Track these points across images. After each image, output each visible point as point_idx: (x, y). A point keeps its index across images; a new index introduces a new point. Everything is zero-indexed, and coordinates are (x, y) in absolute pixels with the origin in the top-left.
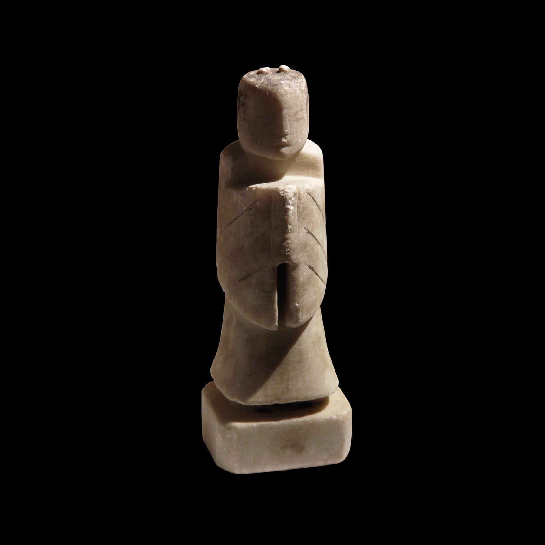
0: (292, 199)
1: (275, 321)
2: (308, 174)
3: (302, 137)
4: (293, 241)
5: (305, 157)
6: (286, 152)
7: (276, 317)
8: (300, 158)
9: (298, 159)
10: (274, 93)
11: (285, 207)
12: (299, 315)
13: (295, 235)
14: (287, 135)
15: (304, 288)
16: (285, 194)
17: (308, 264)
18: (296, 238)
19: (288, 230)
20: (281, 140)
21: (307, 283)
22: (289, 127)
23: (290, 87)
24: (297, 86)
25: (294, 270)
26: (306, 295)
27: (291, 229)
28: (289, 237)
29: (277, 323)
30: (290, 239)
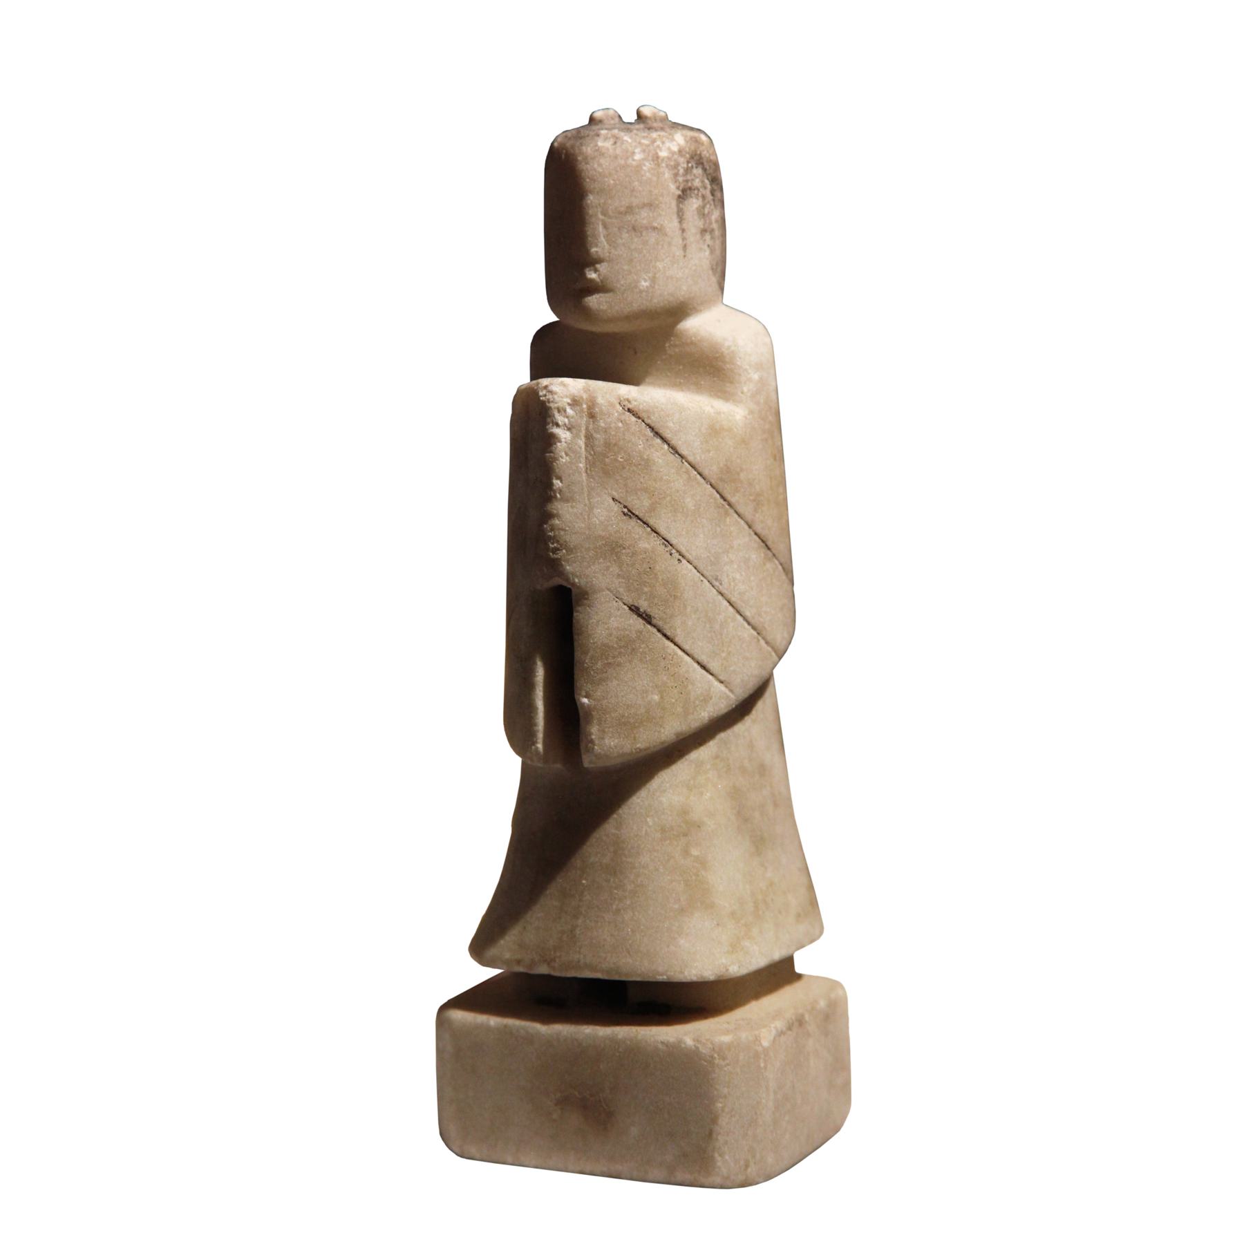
0: (565, 411)
1: (535, 739)
2: (699, 389)
3: (654, 277)
4: (570, 525)
5: (689, 341)
6: (597, 307)
7: (536, 728)
8: (677, 343)
9: (671, 345)
10: (573, 155)
11: (547, 430)
12: (592, 731)
13: (575, 510)
14: (600, 261)
15: (610, 660)
16: (550, 396)
17: (630, 602)
18: (578, 518)
19: (555, 492)
20: (583, 275)
21: (622, 650)
22: (605, 244)
23: (615, 143)
24: (640, 143)
25: (579, 606)
26: (615, 682)
27: (560, 491)
28: (555, 512)
29: (540, 746)
30: (558, 516)
